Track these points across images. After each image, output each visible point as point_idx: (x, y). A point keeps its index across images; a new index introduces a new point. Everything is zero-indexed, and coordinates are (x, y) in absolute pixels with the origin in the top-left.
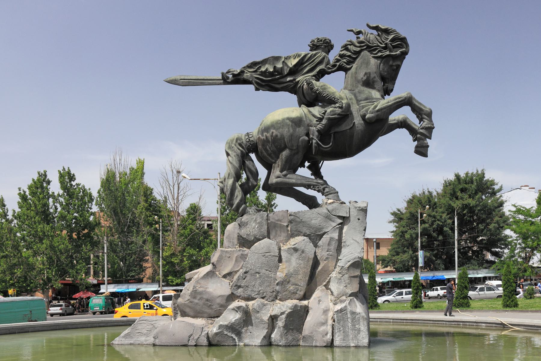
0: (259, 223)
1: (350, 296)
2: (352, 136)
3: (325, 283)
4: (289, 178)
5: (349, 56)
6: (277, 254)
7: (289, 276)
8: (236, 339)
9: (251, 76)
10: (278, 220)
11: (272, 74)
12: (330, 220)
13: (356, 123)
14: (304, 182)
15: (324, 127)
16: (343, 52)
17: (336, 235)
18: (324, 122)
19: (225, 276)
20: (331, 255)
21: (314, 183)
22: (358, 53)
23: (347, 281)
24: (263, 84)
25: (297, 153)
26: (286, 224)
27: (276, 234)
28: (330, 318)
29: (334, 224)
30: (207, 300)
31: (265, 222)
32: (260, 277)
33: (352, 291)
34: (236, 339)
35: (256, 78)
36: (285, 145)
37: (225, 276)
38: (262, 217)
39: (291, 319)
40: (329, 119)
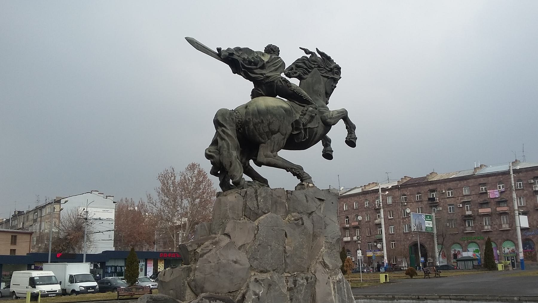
0: (264, 197)
3: (317, 257)
5: (306, 69)
10: (279, 197)
11: (250, 63)
14: (286, 165)
16: (300, 64)
18: (307, 117)
19: (240, 248)
21: (295, 168)
22: (312, 68)
25: (284, 139)
27: (276, 209)
30: (231, 274)
32: (272, 249)
37: (240, 248)
38: (267, 192)
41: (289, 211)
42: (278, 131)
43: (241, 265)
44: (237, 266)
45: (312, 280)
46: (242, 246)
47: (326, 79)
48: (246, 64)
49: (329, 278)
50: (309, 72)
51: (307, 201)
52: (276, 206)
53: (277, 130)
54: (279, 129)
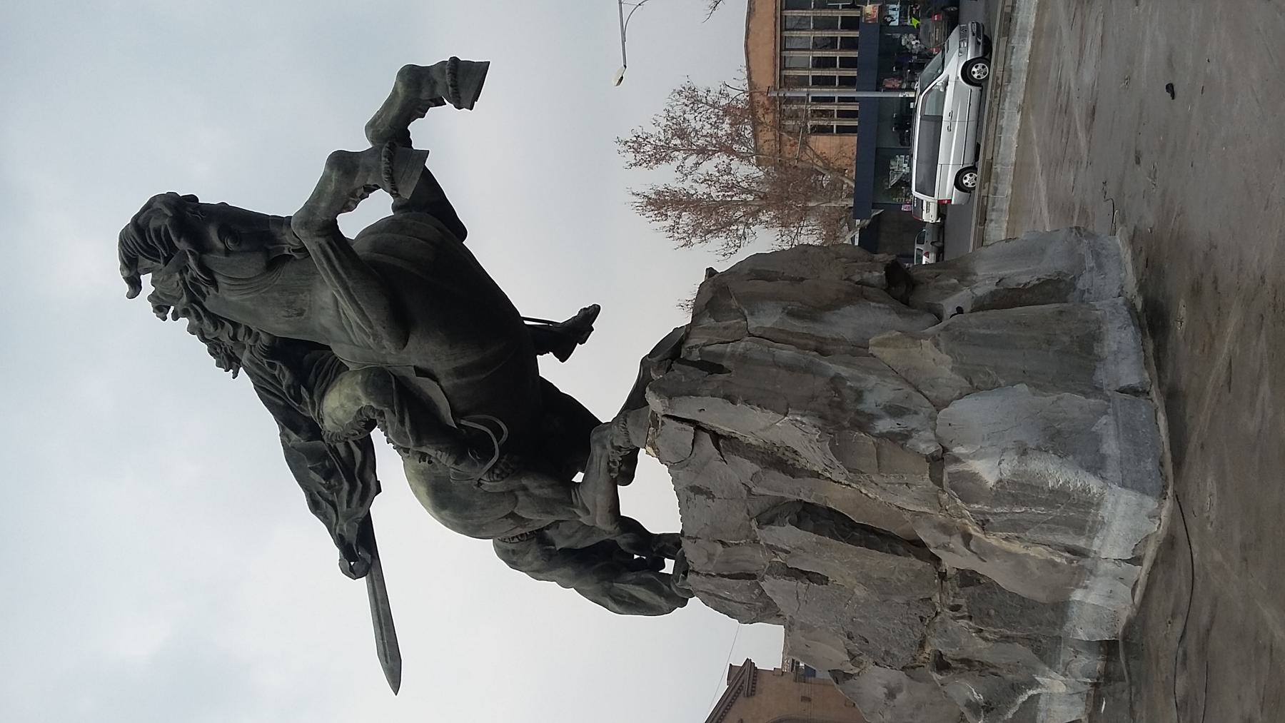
1: (939, 483)
2: (460, 372)
4: (595, 505)
6: (802, 586)
7: (866, 580)
8: (1031, 692)
9: (347, 517)
12: (705, 464)
13: (418, 364)
15: (446, 450)
17: (750, 467)
20: (811, 490)
22: (217, 321)
23: (892, 479)
24: (360, 485)
25: (525, 489)
26: (720, 547)
28: (1005, 545)
29: (716, 463)
30: (918, 708)
31: (718, 580)
33: (927, 476)
34: (1031, 692)
35: (348, 506)
36: (506, 517)
39: (992, 612)
40: (419, 442)
41: (747, 537)
42: (512, 515)
43: (900, 690)
44: (901, 697)
45: (962, 602)
46: (853, 657)
47: (220, 279)
48: (341, 483)
49: (967, 538)
50: (236, 325)
51: (709, 495)
52: (738, 560)
53: (511, 521)
54: (506, 517)
